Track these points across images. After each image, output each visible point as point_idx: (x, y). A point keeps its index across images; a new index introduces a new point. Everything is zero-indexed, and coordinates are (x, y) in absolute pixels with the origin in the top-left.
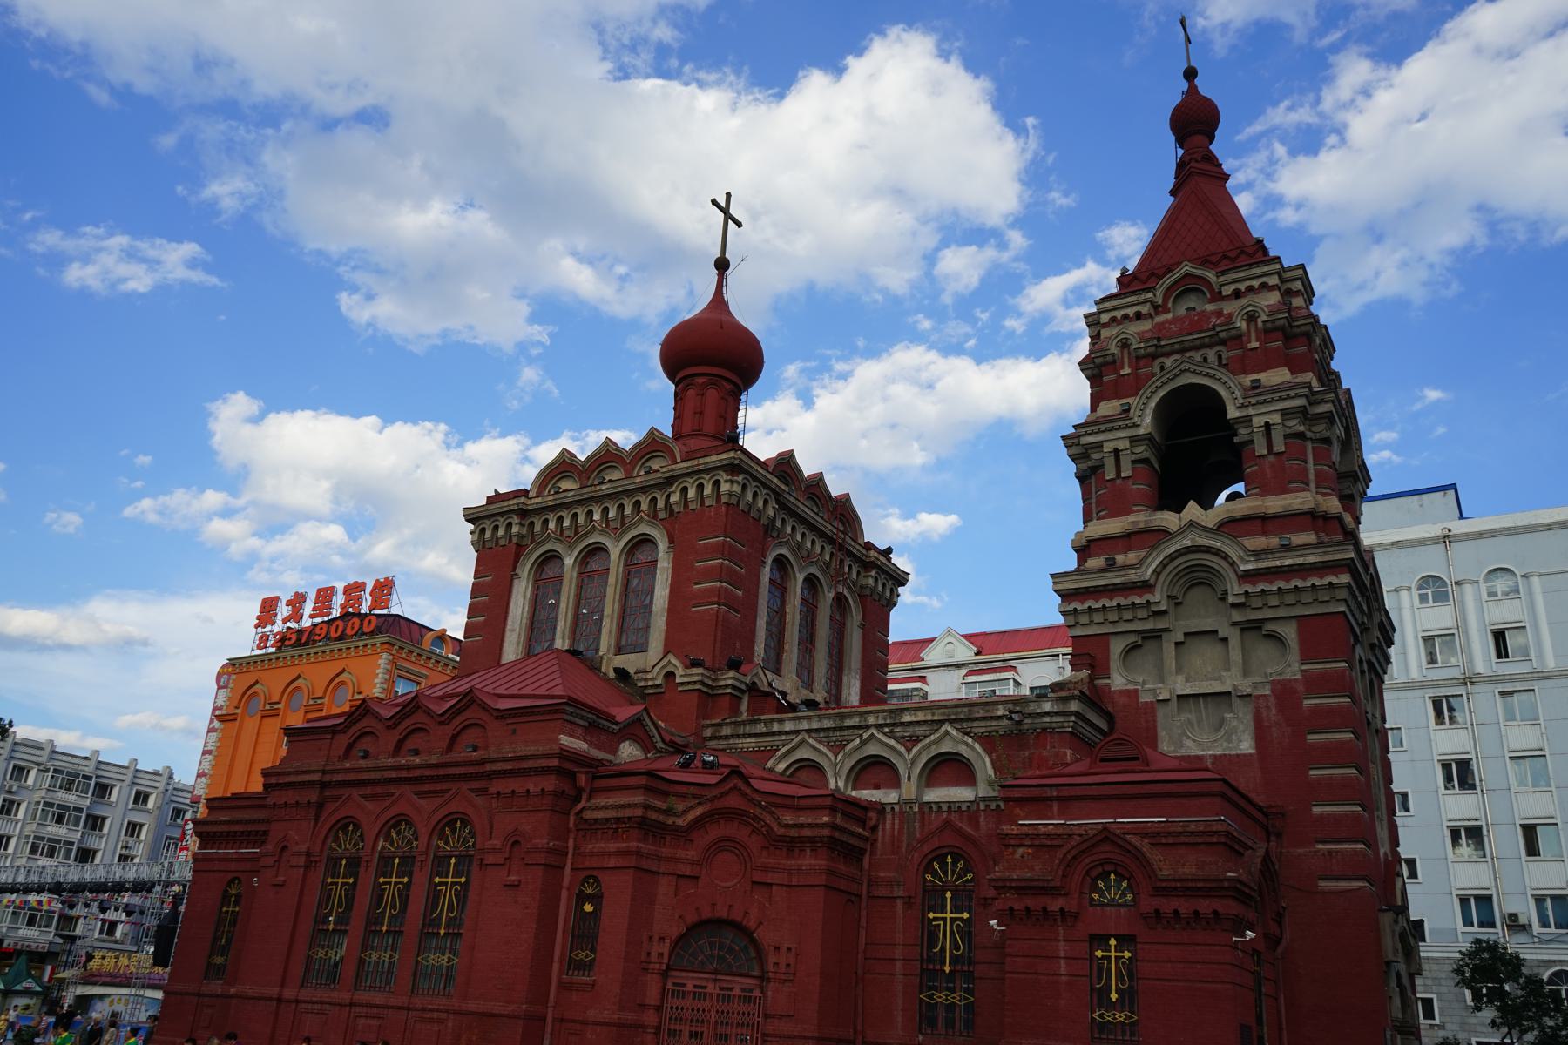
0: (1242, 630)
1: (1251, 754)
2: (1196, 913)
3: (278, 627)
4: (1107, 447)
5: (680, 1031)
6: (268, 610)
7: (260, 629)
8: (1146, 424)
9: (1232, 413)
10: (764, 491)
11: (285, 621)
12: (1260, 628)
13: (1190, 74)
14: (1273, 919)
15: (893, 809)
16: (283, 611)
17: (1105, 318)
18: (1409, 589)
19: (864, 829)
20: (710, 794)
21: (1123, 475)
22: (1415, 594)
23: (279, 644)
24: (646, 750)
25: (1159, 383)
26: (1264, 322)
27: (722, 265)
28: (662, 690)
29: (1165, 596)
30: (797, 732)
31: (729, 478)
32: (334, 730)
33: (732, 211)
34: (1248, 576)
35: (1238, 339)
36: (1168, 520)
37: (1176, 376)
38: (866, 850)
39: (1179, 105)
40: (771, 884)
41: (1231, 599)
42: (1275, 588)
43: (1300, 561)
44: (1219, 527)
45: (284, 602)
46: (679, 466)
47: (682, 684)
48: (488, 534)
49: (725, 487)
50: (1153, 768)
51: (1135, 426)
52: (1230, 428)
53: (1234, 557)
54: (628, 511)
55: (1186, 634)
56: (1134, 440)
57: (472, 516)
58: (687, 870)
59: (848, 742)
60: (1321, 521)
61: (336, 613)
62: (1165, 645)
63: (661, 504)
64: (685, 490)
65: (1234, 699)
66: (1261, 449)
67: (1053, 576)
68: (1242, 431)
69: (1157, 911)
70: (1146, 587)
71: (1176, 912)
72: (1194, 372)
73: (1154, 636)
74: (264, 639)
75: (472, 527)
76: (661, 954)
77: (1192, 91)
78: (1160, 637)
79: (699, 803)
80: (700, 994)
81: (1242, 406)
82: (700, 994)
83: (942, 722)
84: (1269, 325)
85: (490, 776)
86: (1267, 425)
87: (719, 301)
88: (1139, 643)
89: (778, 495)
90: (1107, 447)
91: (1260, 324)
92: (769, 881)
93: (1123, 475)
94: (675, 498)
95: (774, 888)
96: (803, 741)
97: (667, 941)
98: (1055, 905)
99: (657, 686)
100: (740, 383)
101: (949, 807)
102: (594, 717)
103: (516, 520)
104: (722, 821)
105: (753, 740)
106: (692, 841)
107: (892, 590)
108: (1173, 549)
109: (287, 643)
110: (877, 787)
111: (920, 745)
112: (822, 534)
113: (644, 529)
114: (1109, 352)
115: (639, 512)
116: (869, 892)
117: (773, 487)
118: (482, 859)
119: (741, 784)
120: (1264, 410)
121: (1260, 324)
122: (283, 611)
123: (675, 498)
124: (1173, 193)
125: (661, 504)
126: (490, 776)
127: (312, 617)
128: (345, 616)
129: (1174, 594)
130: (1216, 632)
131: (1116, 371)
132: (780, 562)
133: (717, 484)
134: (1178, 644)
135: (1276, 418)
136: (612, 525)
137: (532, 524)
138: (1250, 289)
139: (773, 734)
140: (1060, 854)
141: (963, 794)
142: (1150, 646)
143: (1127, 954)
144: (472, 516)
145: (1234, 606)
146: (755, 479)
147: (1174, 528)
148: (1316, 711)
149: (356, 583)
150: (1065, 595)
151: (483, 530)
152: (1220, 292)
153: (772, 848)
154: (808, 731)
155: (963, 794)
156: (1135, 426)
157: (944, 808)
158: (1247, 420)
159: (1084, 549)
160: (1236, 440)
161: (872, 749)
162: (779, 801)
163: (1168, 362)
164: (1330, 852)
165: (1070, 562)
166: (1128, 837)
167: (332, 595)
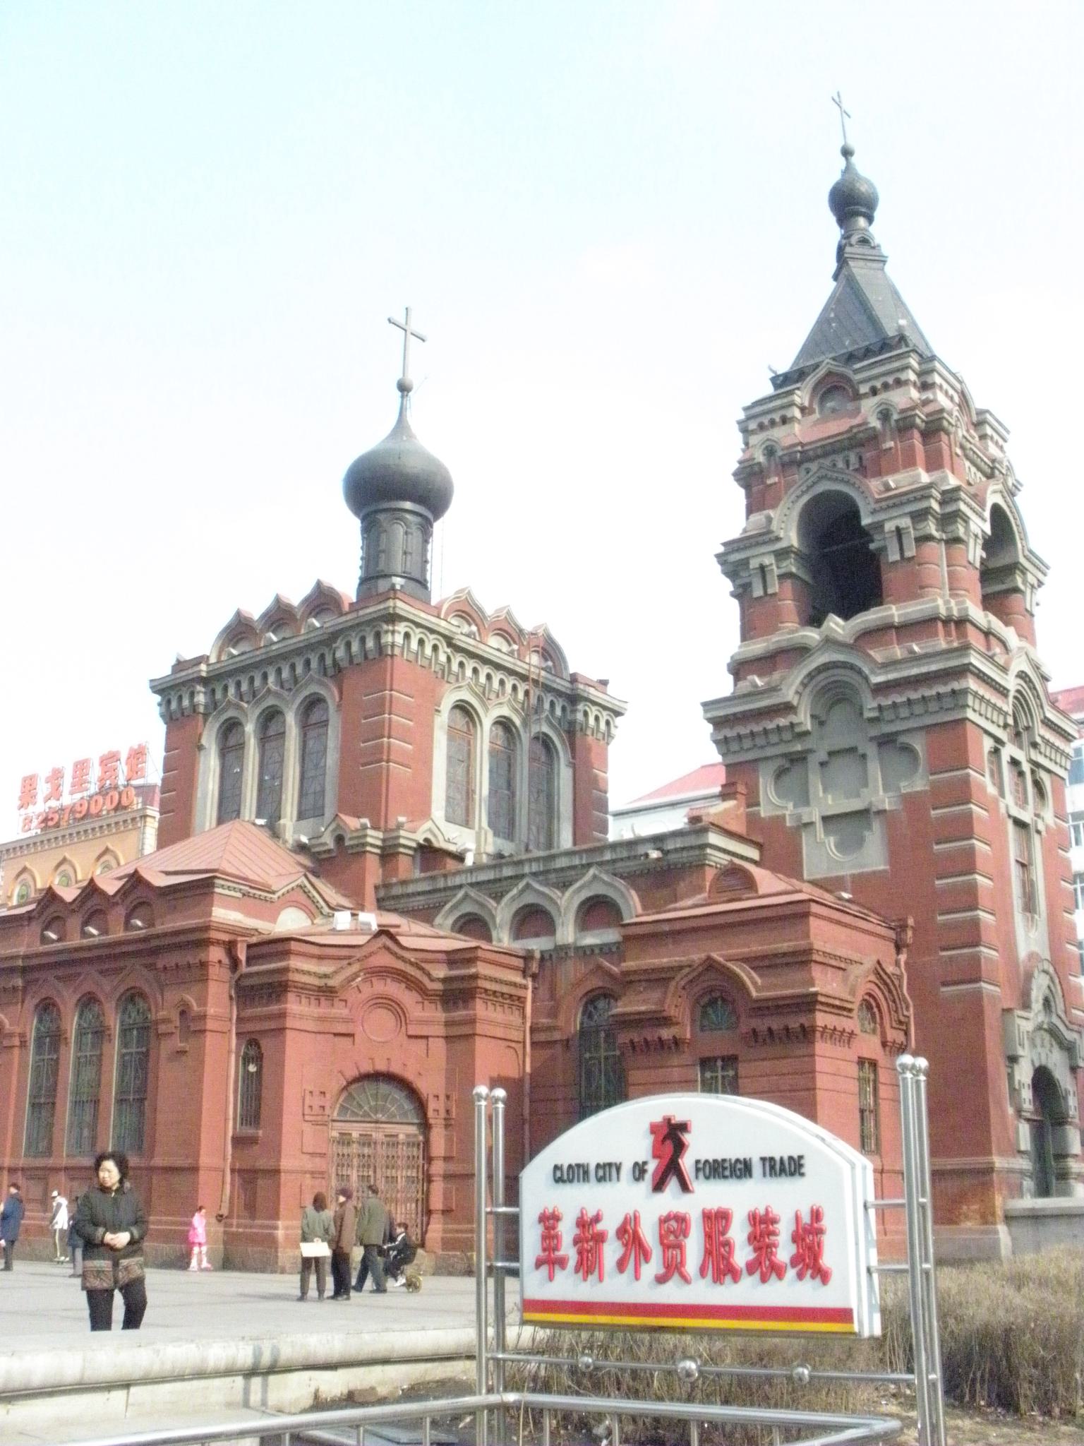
0: (880, 745)
1: (885, 871)
2: (787, 1029)
3: (40, 807)
4: (754, 564)
5: (348, 1176)
6: (29, 786)
7: (23, 811)
8: (791, 537)
9: (866, 521)
10: (432, 637)
11: (47, 799)
12: (894, 741)
14: (892, 1027)
15: (551, 956)
16: (43, 789)
17: (753, 425)
19: (524, 977)
20: (358, 954)
21: (770, 591)
23: (43, 825)
24: (312, 916)
25: (799, 493)
26: (897, 421)
28: (334, 855)
29: (808, 716)
30: (460, 887)
31: (391, 628)
32: (29, 917)
33: (414, 326)
34: (880, 689)
35: (873, 438)
36: (812, 635)
37: (814, 483)
38: (525, 998)
39: (838, 183)
40: (427, 1037)
41: (868, 714)
42: (890, 703)
43: (924, 669)
44: (856, 640)
45: (43, 780)
46: (343, 619)
47: (352, 847)
48: (174, 705)
49: (388, 639)
50: (761, 892)
52: (865, 535)
53: (866, 670)
54: (299, 669)
55: (831, 754)
56: (781, 554)
58: (341, 1028)
59: (507, 892)
60: (953, 626)
61: (93, 788)
62: (810, 765)
63: (329, 661)
64: (348, 645)
65: (872, 816)
66: (894, 556)
67: (705, 705)
68: (876, 537)
69: (754, 1031)
70: (788, 708)
71: (770, 1029)
72: (830, 479)
73: (798, 759)
74: (27, 821)
75: (158, 698)
76: (323, 1107)
77: (848, 169)
78: (805, 759)
79: (349, 964)
80: (366, 1141)
81: (874, 512)
82: (366, 1141)
83: (589, 865)
84: (901, 423)
85: (155, 952)
86: (899, 532)
87: (401, 426)
88: (787, 766)
89: (450, 642)
90: (754, 564)
91: (893, 423)
92: (425, 1034)
93: (770, 591)
94: (340, 653)
95: (430, 1039)
96: (466, 896)
97: (328, 1095)
98: (666, 1033)
99: (329, 851)
100: (430, 516)
101: (601, 949)
102: (247, 888)
103: (199, 688)
104: (374, 980)
105: (421, 898)
106: (346, 1001)
107: (608, 723)
108: (814, 665)
109: (50, 823)
110: (537, 935)
111: (571, 889)
112: (512, 672)
113: (314, 688)
114: (756, 461)
115: (309, 669)
116: (531, 1039)
117: (442, 630)
118: (157, 1029)
119: (389, 943)
120: (896, 514)
121: (893, 423)
122: (43, 789)
123: (340, 653)
124: (836, 277)
125: (329, 661)
126: (155, 952)
127: (72, 793)
128: (103, 792)
129: (817, 713)
130: (852, 750)
131: (763, 482)
132: (463, 708)
133: (378, 636)
134: (822, 764)
135: (905, 522)
136: (287, 686)
137: (213, 691)
138: (886, 386)
139: (439, 890)
140: (673, 983)
141: (610, 936)
142: (797, 771)
143: (731, 1073)
145: (871, 720)
146: (418, 625)
147: (813, 644)
148: (943, 820)
149: (109, 752)
150: (718, 723)
151: (169, 702)
152: (858, 391)
153: (426, 1002)
154: (472, 885)
155: (610, 936)
156: (778, 539)
157: (597, 951)
158: (879, 526)
159: (739, 669)
160: (872, 546)
161: (529, 898)
162: (430, 956)
163: (814, 466)
164: (951, 957)
165: (725, 686)
166: (729, 964)
167: (88, 767)
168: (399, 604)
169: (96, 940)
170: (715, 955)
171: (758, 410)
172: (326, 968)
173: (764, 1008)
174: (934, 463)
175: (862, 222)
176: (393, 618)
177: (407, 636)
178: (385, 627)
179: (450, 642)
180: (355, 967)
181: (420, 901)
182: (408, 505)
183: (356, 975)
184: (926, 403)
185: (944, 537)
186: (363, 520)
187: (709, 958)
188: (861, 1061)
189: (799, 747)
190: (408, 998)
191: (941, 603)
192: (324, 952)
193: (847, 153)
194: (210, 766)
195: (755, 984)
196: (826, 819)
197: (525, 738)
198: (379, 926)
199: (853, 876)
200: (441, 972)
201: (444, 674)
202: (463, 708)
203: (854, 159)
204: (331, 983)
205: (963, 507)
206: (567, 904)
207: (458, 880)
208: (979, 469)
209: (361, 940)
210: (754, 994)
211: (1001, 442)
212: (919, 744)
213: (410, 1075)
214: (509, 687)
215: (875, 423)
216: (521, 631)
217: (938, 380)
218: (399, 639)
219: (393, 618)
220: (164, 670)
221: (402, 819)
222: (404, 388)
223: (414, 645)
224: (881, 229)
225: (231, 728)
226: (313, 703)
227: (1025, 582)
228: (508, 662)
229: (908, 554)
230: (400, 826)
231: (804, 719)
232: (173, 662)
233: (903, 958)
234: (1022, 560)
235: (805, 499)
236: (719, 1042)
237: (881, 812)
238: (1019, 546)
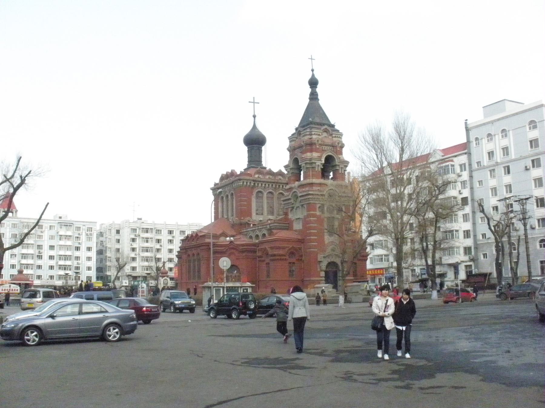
10: (249, 181)
13: (313, 70)
18: (484, 138)
22: (486, 139)
27: (254, 117)
30: (249, 231)
34: (301, 196)
51: (290, 166)
55: (297, 207)
57: (212, 189)
70: (289, 199)
73: (293, 208)
75: (212, 191)
77: (313, 75)
81: (301, 162)
87: (254, 127)
144: (212, 189)
146: (246, 180)
158: (301, 165)
168: (240, 177)
169: (194, 244)
170: (267, 247)
171: (292, 137)
172: (222, 249)
173: (272, 256)
174: (311, 151)
175: (314, 88)
176: (240, 180)
177: (243, 182)
178: (239, 181)
179: (254, 181)
180: (227, 248)
181: (245, 233)
182: (255, 146)
183: (227, 250)
184: (311, 138)
185: (311, 166)
186: (248, 148)
187: (265, 248)
188: (290, 263)
189: (292, 206)
190: (236, 253)
191: (308, 181)
192: (221, 246)
193: (313, 70)
194: (220, 204)
195: (270, 252)
196: (296, 219)
197: (276, 194)
198: (234, 239)
199: (299, 230)
200: (241, 248)
201: (254, 187)
202: (260, 192)
203: (314, 72)
204: (224, 251)
205: (313, 161)
206: (260, 234)
207: (249, 230)
208: (328, 146)
209: (228, 243)
210: (270, 253)
211: (339, 136)
212: (305, 206)
213: (237, 265)
214: (270, 185)
215: (303, 144)
216: (274, 173)
217: (313, 133)
218: (241, 183)
219: (240, 180)
220: (213, 186)
221: (242, 218)
222: (254, 117)
223: (245, 184)
224: (319, 90)
225: (222, 198)
226: (232, 194)
227: (339, 168)
228: (269, 180)
229: (305, 171)
230: (243, 219)
231: (292, 201)
232: (214, 184)
233: (302, 245)
234: (337, 164)
235: (293, 159)
236: (267, 261)
237: (301, 219)
238: (337, 161)
